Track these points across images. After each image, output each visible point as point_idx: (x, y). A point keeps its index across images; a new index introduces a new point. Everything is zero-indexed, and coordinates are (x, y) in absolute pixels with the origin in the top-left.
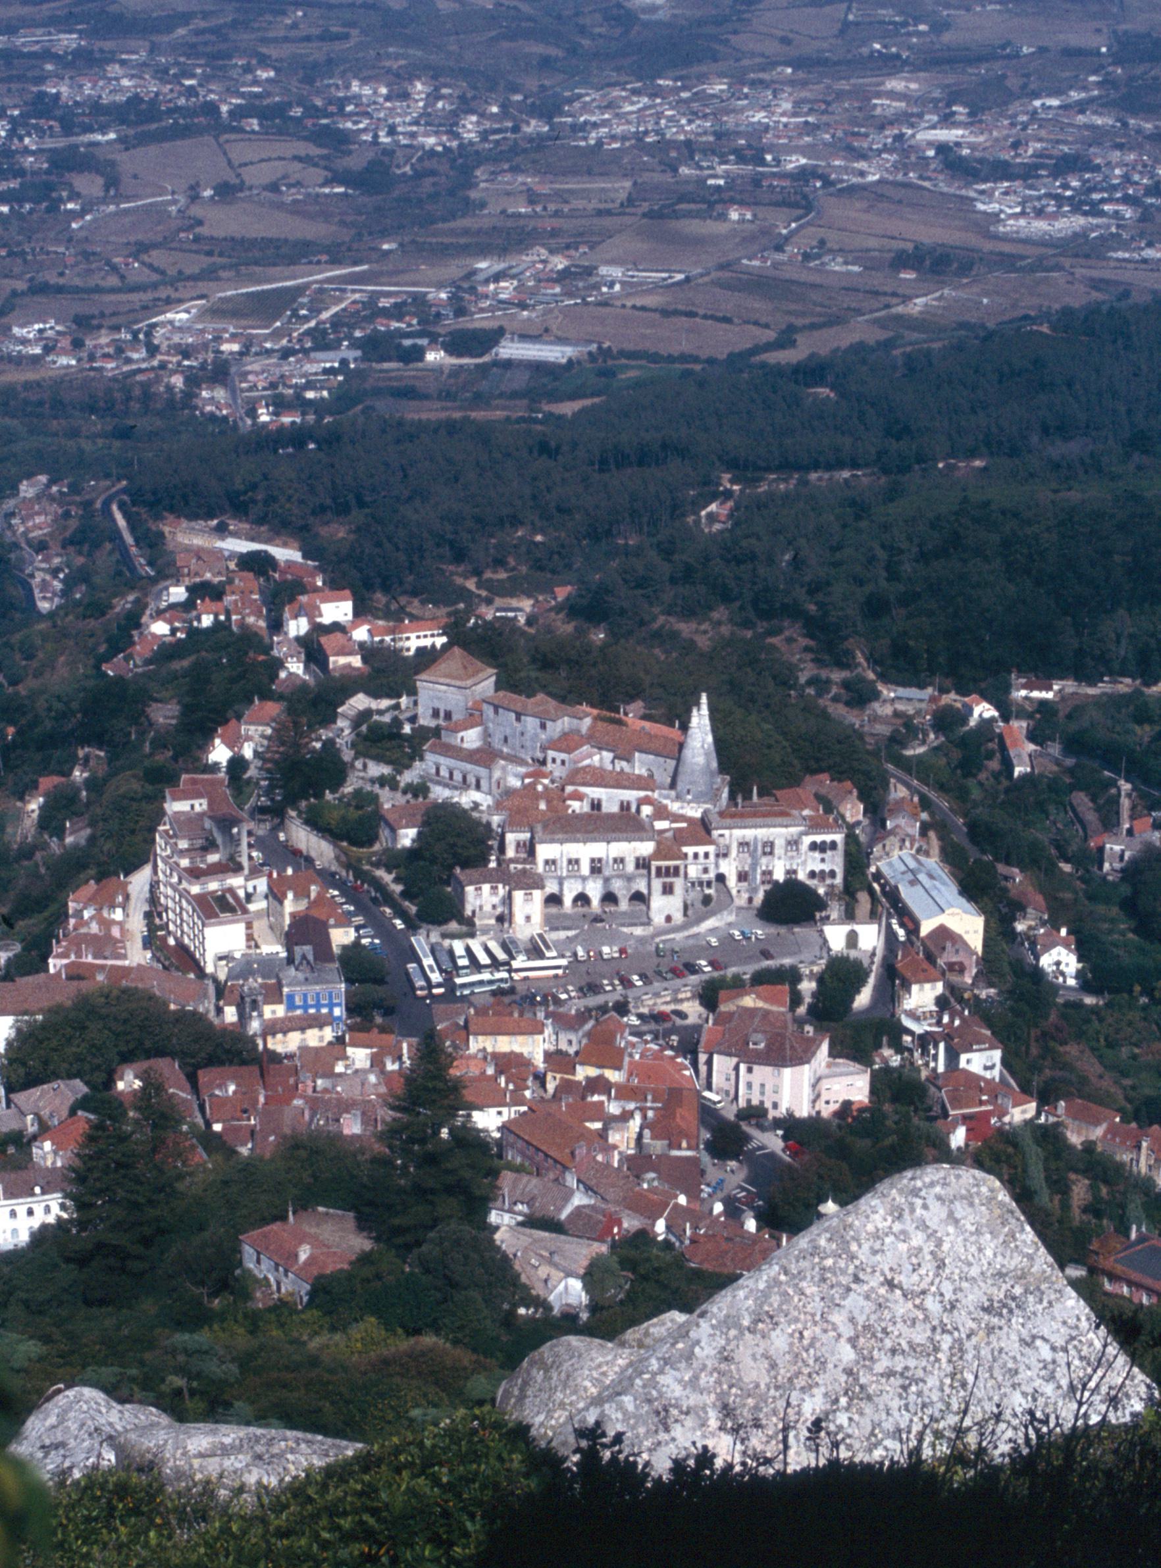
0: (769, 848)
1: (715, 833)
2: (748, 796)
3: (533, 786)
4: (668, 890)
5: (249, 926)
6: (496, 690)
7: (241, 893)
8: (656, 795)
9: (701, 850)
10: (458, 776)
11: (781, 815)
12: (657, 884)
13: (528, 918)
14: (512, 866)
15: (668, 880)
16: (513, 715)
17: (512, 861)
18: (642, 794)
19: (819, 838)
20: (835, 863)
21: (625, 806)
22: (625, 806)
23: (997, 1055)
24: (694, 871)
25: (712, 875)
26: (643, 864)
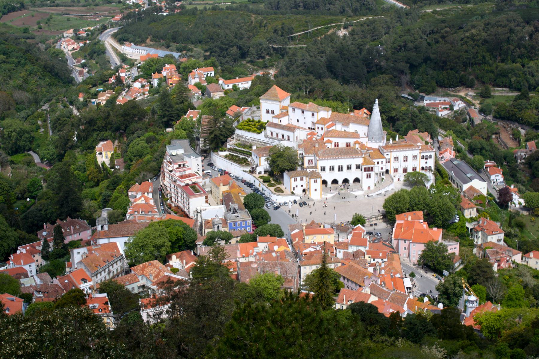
0: (406, 159)
1: (385, 155)
2: (394, 139)
3: (311, 139)
4: (369, 176)
5: (206, 197)
6: (291, 102)
7: (201, 184)
8: (358, 140)
9: (380, 161)
10: (280, 137)
11: (410, 146)
12: (365, 174)
13: (316, 190)
14: (308, 170)
15: (368, 173)
16: (301, 111)
17: (308, 167)
18: (355, 140)
19: (425, 154)
20: (431, 163)
21: (348, 145)
22: (348, 145)
23: (502, 236)
24: (377, 169)
25: (384, 170)
26: (358, 167)
